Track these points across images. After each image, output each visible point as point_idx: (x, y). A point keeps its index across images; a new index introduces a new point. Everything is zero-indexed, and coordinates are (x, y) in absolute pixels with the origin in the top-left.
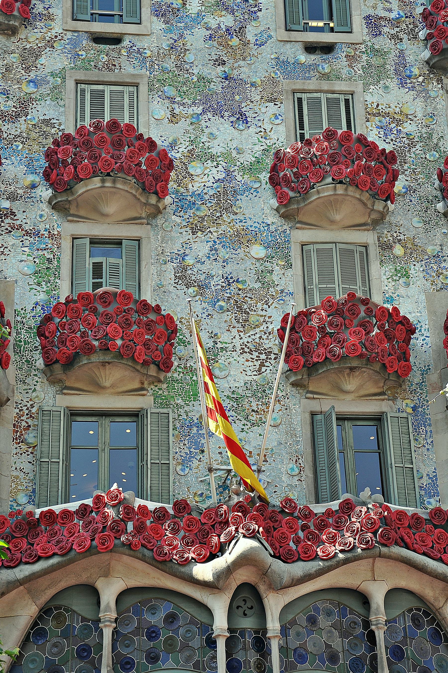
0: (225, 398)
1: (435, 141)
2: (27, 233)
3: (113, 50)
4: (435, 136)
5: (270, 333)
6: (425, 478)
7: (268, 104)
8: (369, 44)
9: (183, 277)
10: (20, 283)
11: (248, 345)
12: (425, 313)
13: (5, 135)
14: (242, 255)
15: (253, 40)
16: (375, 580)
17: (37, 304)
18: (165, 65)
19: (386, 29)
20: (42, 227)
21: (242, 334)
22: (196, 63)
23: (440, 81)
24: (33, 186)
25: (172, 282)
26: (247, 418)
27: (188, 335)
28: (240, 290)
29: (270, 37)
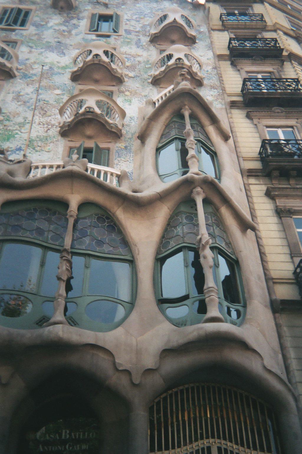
0: (24, 140)
5: (56, 119)
11: (43, 122)
16: (72, 193)
19: (133, 33)
21: (41, 118)
23: (154, 46)
26: (34, 149)
27: (12, 119)
28: (44, 103)
29: (82, 33)
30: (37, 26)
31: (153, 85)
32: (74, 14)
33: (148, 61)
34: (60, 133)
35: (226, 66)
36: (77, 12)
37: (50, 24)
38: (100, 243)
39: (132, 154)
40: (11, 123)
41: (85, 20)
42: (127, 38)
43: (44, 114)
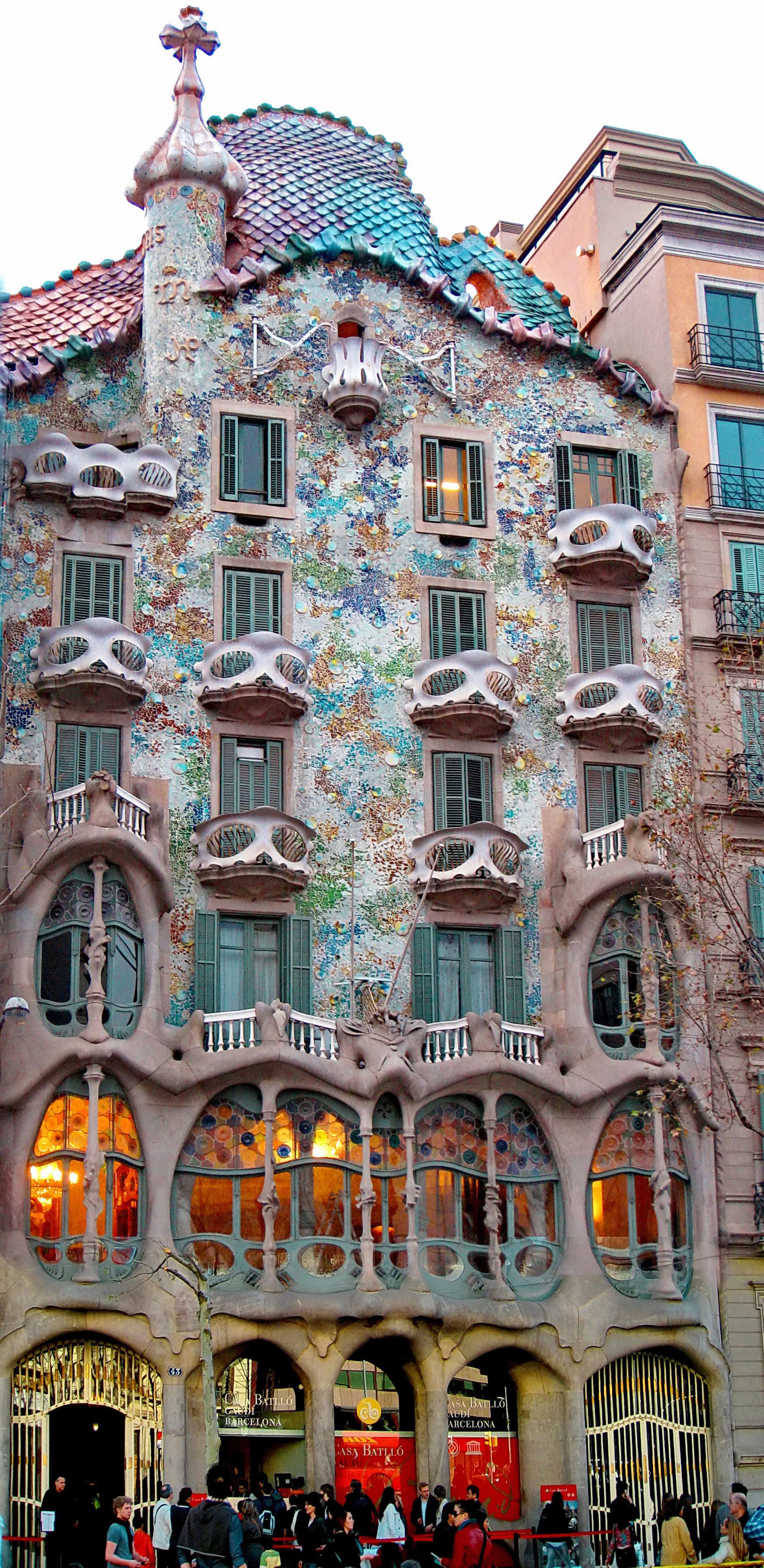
1: (558, 650)
2: (179, 730)
3: (259, 535)
4: (558, 644)
6: (530, 988)
7: (406, 601)
8: (502, 541)
9: (322, 782)
10: (174, 782)
12: (540, 828)
13: (156, 624)
14: (377, 762)
15: (391, 530)
17: (189, 804)
18: (308, 553)
19: (517, 526)
20: (192, 724)
22: (337, 551)
23: (564, 586)
24: (183, 680)
25: (313, 787)
26: (378, 927)
27: (326, 842)
30: (309, 495)
31: (567, 735)
32: (380, 438)
33: (553, 646)
34: (415, 889)
35: (705, 662)
36: (386, 426)
37: (336, 489)
38: (522, 1161)
39: (536, 942)
40: (328, 854)
41: (409, 467)
42: (505, 548)
43: (379, 829)
